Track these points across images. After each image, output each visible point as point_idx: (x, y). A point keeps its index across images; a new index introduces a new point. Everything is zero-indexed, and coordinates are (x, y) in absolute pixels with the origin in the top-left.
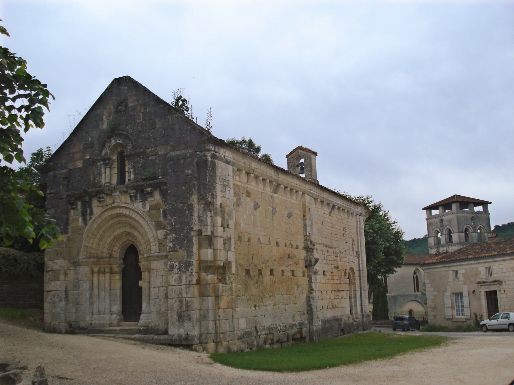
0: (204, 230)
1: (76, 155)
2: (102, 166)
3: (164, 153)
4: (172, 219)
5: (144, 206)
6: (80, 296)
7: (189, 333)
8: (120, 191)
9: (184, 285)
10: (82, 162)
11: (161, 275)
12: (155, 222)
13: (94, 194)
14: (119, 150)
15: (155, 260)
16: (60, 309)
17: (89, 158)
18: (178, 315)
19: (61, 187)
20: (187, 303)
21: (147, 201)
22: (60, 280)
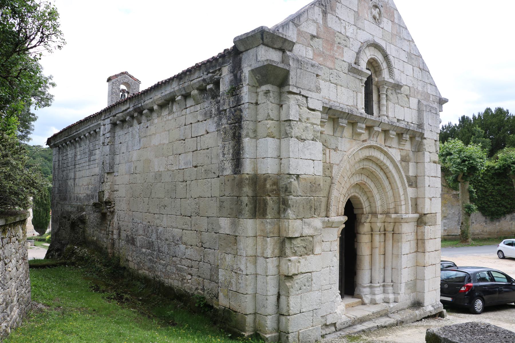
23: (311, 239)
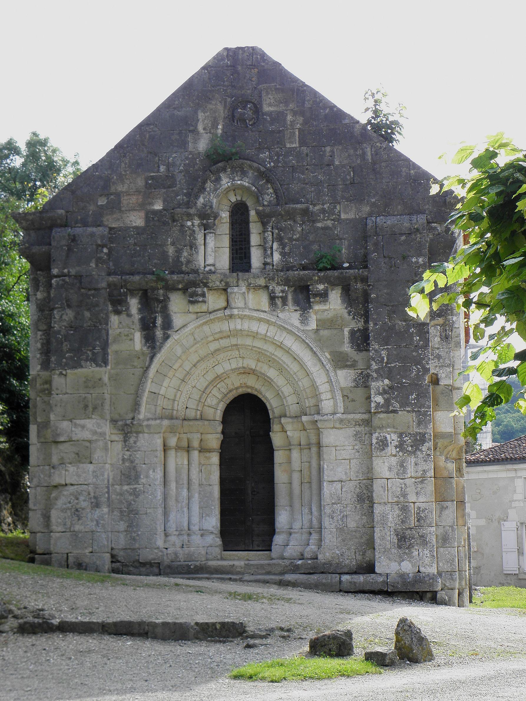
0: (443, 375)
1: (125, 198)
2: (196, 229)
3: (353, 216)
4: (383, 350)
5: (304, 320)
6: (141, 497)
7: (422, 569)
8: (249, 284)
9: (411, 477)
10: (142, 214)
11: (348, 458)
12: (331, 353)
13: (180, 286)
14: (233, 199)
15: (334, 428)
16: (95, 523)
17: (162, 208)
18: (397, 535)
19: (93, 265)
20: (419, 513)
21: (311, 310)
22: (93, 462)
23: (88, 444)
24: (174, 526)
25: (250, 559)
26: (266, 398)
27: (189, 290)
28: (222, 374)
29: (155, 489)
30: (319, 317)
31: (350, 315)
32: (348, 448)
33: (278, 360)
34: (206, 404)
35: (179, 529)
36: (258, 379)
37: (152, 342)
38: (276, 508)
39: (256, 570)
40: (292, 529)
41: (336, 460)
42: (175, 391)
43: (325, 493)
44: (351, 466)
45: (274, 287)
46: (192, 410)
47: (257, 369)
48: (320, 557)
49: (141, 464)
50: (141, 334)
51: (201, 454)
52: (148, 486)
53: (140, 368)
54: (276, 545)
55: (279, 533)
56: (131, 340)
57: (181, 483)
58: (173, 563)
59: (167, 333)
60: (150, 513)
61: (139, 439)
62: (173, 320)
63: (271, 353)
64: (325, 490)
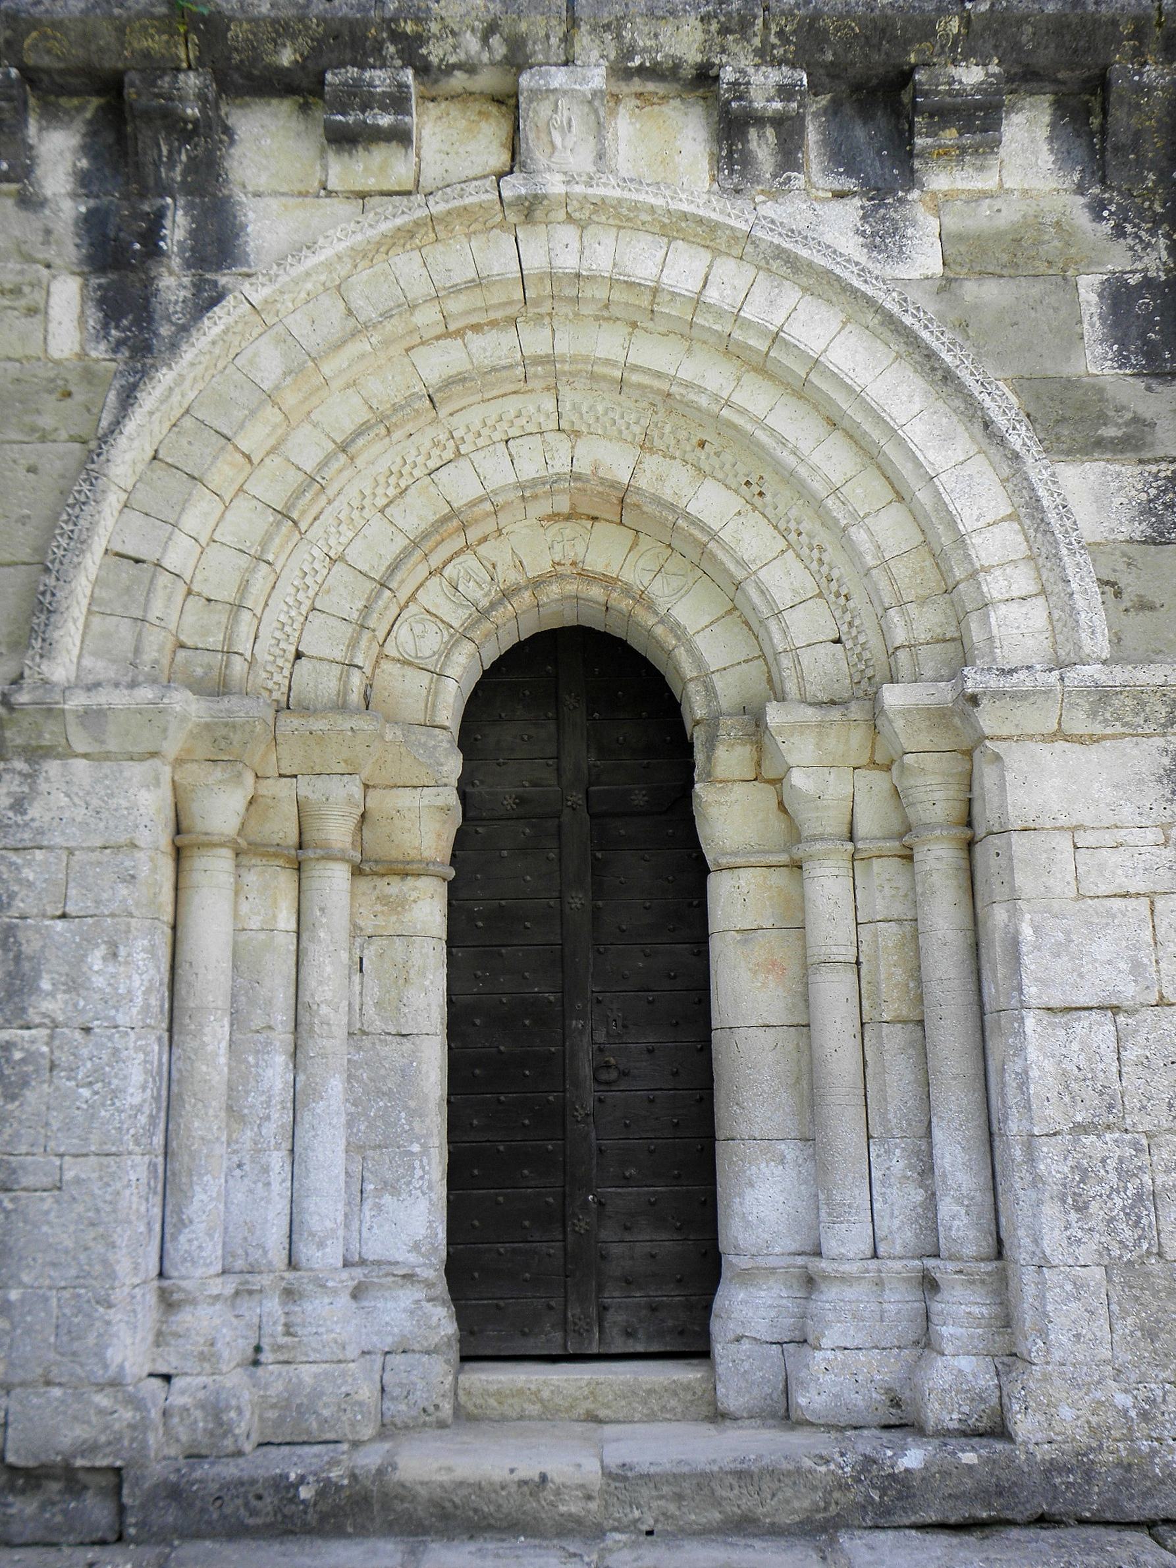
12: (1021, 384)
15: (1060, 735)
21: (914, 195)
24: (213, 1253)
25: (602, 1413)
26: (676, 629)
27: (329, 76)
28: (473, 504)
29: (116, 1051)
30: (952, 223)
31: (1099, 218)
32: (1135, 837)
33: (749, 427)
34: (390, 649)
35: (239, 1264)
36: (635, 544)
37: (137, 322)
38: (720, 1147)
39: (672, 1508)
40: (819, 1254)
41: (1080, 897)
42: (244, 561)
43: (1034, 1073)
44: (1162, 931)
45: (742, 72)
46: (326, 666)
47: (643, 482)
48: (1025, 1426)
49: (44, 916)
50: (85, 286)
51: (364, 884)
52: (78, 1035)
53: (73, 439)
54: (738, 1340)
55: (748, 1277)
56: (32, 311)
57: (258, 1022)
58: (204, 1470)
59: (215, 283)
60: (78, 1181)
61: (43, 786)
62: (243, 227)
63: (716, 398)
64: (1033, 1054)
